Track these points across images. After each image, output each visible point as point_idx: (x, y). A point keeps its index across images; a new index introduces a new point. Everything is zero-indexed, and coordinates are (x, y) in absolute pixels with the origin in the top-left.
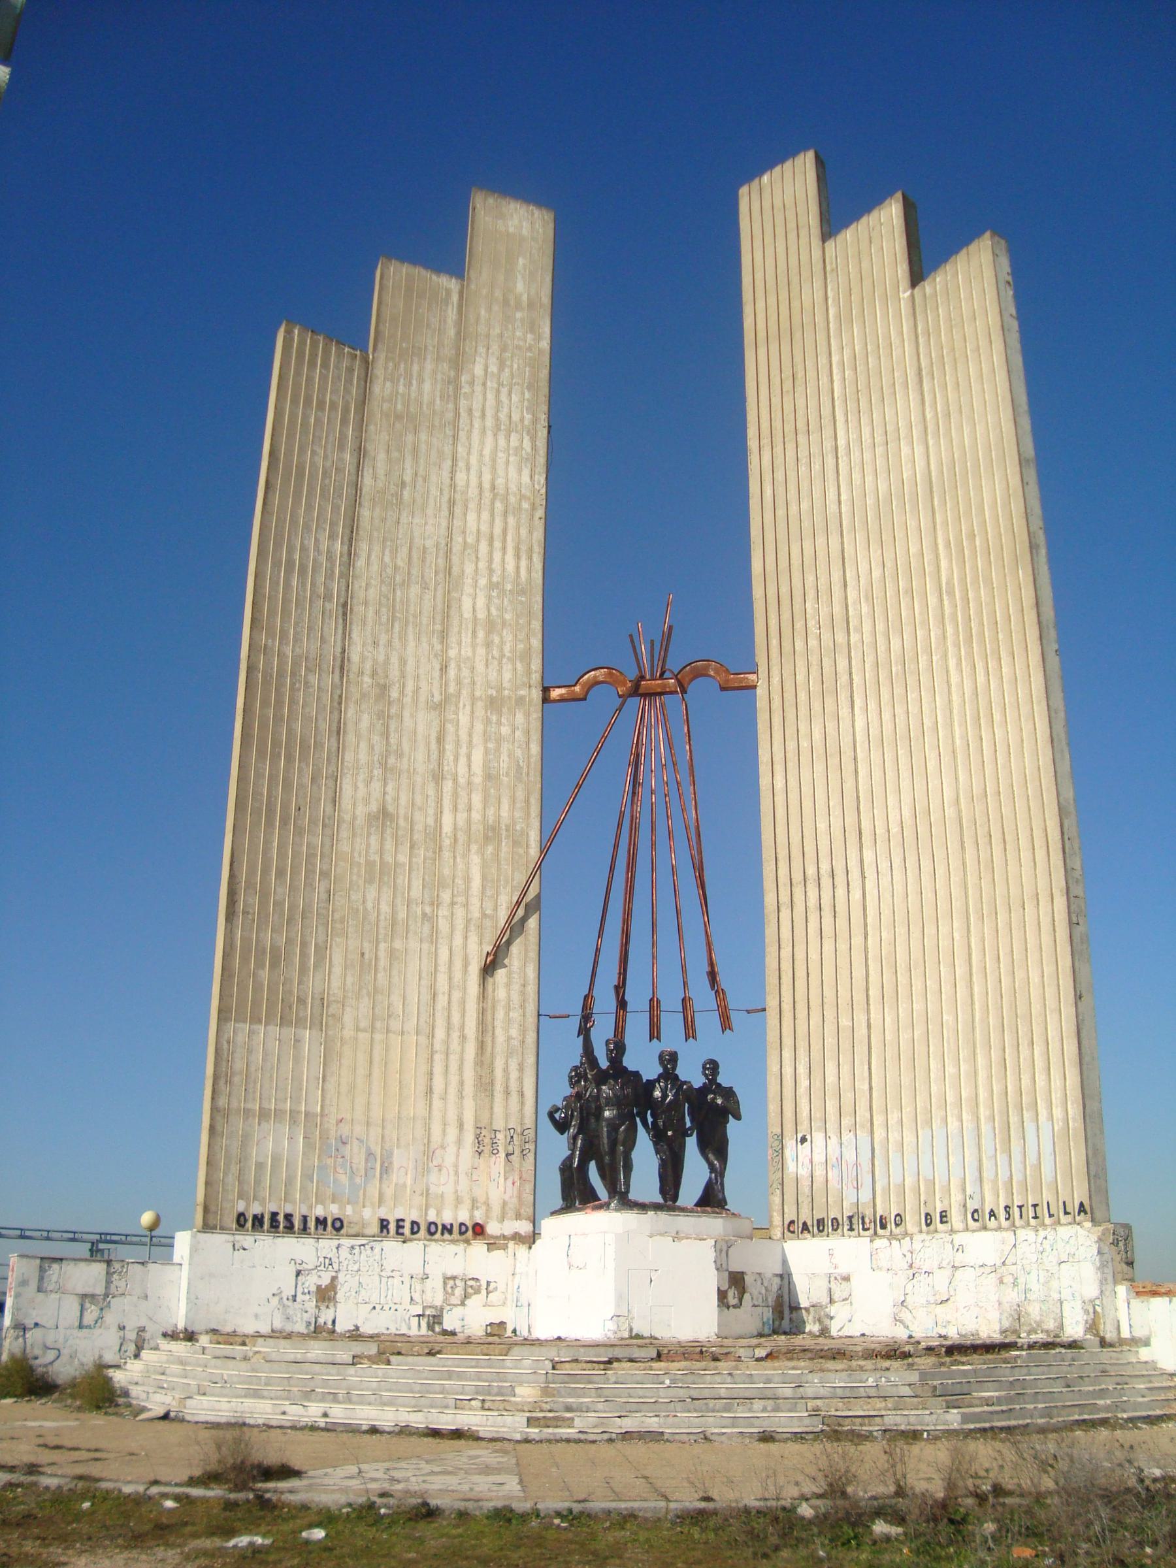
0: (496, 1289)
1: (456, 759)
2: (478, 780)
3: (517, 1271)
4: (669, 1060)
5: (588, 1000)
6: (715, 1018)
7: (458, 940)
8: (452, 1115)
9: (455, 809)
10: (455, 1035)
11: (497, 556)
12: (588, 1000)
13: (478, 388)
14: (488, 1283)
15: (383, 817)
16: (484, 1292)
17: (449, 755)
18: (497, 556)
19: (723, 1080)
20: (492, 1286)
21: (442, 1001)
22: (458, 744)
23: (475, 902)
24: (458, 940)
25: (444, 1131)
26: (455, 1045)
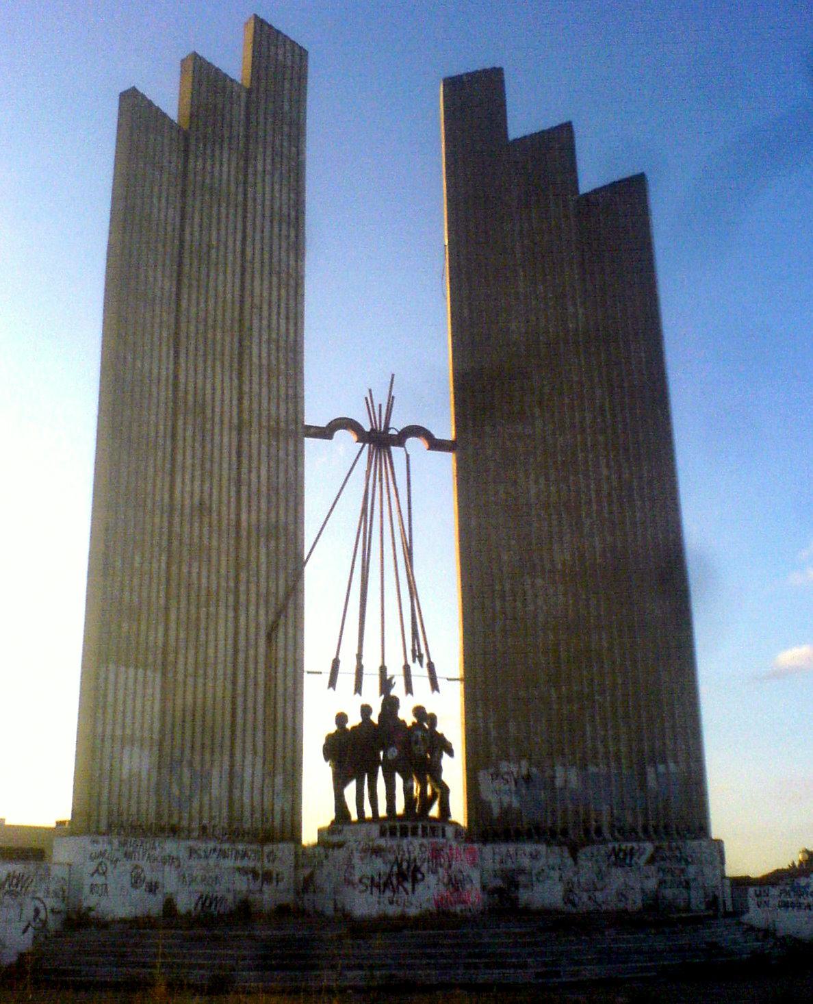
0: (283, 878)
1: (250, 472)
2: (264, 489)
3: (300, 863)
4: (419, 712)
5: (336, 663)
6: (427, 682)
7: (252, 608)
8: (249, 746)
9: (249, 512)
10: (251, 683)
11: (274, 317)
12: (336, 663)
13: (259, 180)
14: (277, 875)
15: (202, 508)
16: (275, 883)
17: (244, 470)
18: (274, 317)
19: (439, 729)
20: (280, 876)
21: (241, 657)
22: (250, 457)
23: (263, 584)
24: (252, 608)
25: (244, 757)
26: (251, 690)
